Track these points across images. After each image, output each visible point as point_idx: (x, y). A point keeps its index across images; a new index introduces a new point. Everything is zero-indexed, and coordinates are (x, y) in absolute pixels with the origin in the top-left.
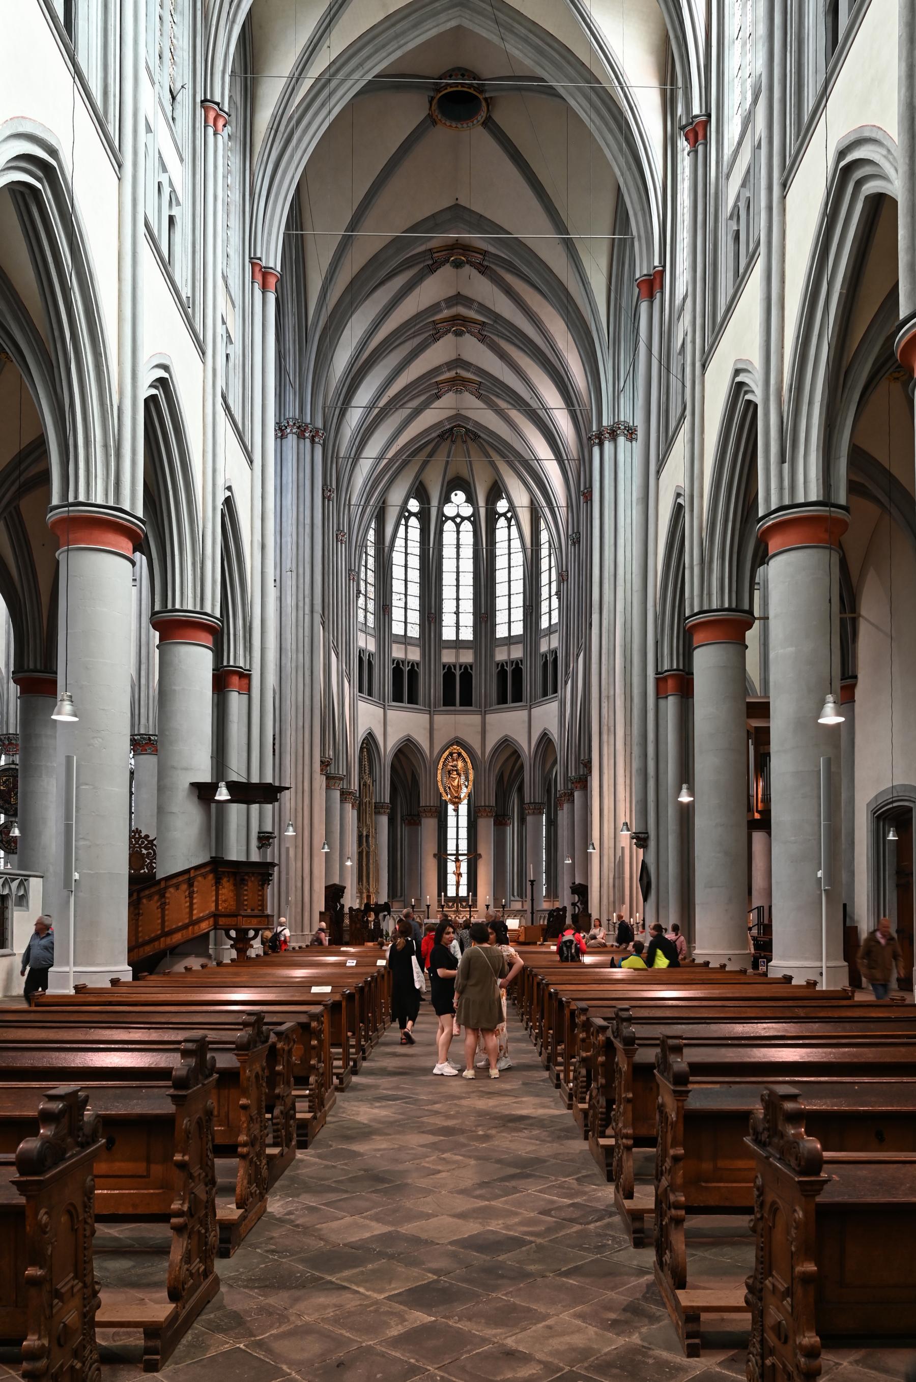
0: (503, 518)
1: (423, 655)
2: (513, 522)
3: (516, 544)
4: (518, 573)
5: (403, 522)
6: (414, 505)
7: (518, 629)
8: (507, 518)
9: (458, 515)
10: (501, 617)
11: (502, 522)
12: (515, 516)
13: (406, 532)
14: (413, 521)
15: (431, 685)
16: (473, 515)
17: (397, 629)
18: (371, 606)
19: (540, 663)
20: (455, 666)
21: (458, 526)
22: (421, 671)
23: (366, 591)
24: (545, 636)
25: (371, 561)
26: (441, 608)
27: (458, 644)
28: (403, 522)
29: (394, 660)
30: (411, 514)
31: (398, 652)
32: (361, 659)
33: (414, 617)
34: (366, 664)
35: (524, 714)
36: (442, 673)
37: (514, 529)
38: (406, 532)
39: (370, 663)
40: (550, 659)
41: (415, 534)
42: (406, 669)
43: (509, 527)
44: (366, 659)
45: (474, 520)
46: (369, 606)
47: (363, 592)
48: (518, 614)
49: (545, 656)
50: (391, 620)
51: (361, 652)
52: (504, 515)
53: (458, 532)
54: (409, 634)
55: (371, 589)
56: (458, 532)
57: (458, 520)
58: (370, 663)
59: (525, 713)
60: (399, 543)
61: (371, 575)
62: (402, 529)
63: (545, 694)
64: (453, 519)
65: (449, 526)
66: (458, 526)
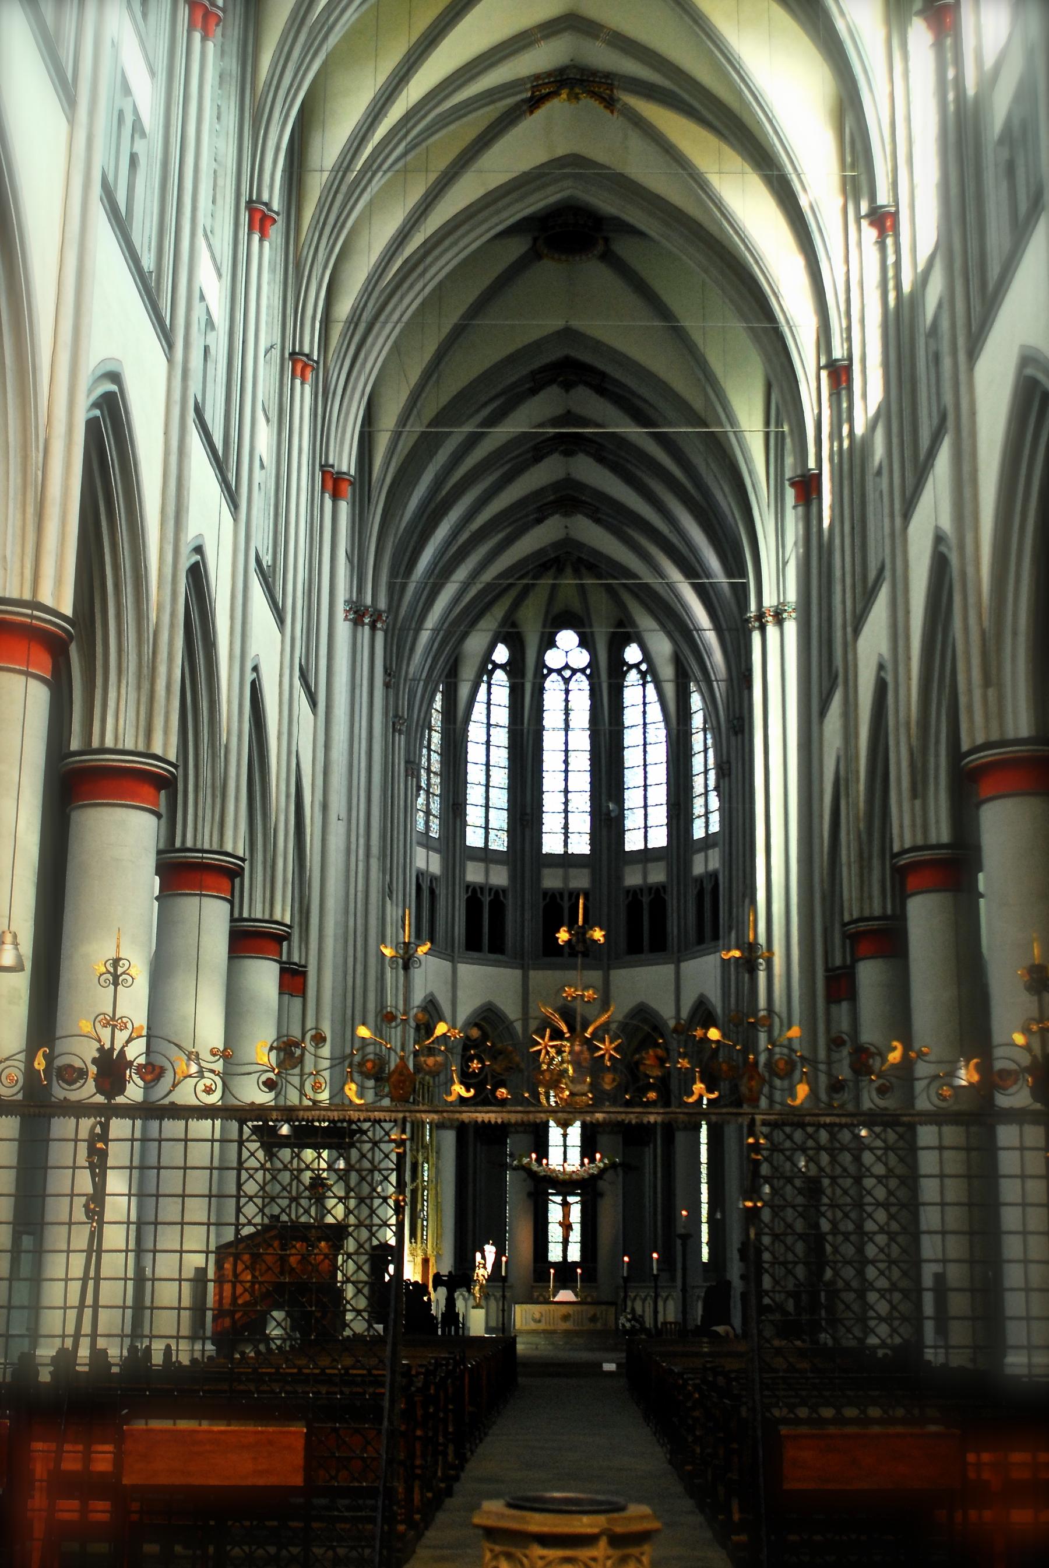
0: (634, 672)
1: (513, 877)
2: (649, 679)
3: (655, 712)
4: (659, 753)
5: (485, 678)
6: (501, 654)
7: (659, 839)
8: (640, 671)
9: (567, 666)
10: (633, 820)
11: (633, 676)
12: (652, 670)
13: (489, 693)
14: (500, 676)
15: (522, 923)
16: (589, 666)
17: (474, 838)
18: (435, 807)
19: (692, 892)
20: (561, 894)
21: (567, 681)
22: (510, 903)
23: (429, 785)
24: (699, 851)
25: (436, 738)
26: (540, 805)
27: (566, 861)
28: (485, 678)
29: (468, 887)
30: (496, 666)
31: (474, 874)
32: (419, 887)
33: (500, 819)
34: (426, 890)
35: (666, 971)
36: (542, 905)
37: (650, 687)
38: (489, 693)
39: (432, 892)
40: (708, 887)
41: (501, 694)
42: (486, 900)
43: (644, 685)
44: (425, 887)
45: (592, 672)
46: (432, 805)
47: (423, 785)
48: (659, 815)
49: (700, 880)
50: (464, 824)
51: (420, 874)
52: (637, 666)
53: (567, 692)
54: (493, 846)
55: (436, 780)
56: (567, 692)
57: (567, 673)
58: (432, 892)
59: (672, 967)
60: (479, 712)
61: (435, 758)
62: (483, 687)
63: (701, 940)
64: (559, 671)
65: (553, 686)
66: (567, 681)
